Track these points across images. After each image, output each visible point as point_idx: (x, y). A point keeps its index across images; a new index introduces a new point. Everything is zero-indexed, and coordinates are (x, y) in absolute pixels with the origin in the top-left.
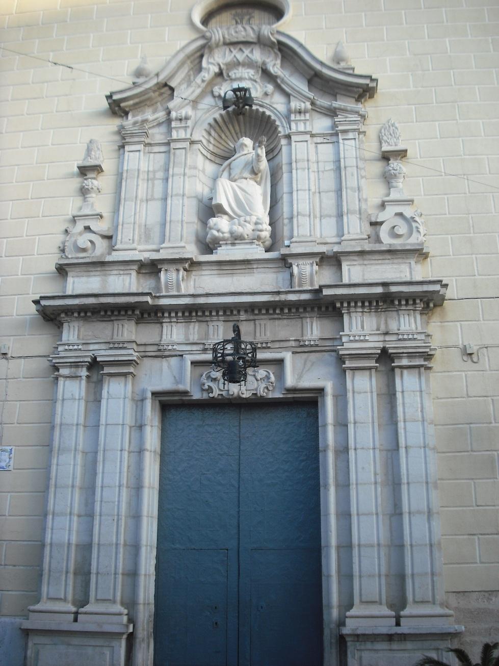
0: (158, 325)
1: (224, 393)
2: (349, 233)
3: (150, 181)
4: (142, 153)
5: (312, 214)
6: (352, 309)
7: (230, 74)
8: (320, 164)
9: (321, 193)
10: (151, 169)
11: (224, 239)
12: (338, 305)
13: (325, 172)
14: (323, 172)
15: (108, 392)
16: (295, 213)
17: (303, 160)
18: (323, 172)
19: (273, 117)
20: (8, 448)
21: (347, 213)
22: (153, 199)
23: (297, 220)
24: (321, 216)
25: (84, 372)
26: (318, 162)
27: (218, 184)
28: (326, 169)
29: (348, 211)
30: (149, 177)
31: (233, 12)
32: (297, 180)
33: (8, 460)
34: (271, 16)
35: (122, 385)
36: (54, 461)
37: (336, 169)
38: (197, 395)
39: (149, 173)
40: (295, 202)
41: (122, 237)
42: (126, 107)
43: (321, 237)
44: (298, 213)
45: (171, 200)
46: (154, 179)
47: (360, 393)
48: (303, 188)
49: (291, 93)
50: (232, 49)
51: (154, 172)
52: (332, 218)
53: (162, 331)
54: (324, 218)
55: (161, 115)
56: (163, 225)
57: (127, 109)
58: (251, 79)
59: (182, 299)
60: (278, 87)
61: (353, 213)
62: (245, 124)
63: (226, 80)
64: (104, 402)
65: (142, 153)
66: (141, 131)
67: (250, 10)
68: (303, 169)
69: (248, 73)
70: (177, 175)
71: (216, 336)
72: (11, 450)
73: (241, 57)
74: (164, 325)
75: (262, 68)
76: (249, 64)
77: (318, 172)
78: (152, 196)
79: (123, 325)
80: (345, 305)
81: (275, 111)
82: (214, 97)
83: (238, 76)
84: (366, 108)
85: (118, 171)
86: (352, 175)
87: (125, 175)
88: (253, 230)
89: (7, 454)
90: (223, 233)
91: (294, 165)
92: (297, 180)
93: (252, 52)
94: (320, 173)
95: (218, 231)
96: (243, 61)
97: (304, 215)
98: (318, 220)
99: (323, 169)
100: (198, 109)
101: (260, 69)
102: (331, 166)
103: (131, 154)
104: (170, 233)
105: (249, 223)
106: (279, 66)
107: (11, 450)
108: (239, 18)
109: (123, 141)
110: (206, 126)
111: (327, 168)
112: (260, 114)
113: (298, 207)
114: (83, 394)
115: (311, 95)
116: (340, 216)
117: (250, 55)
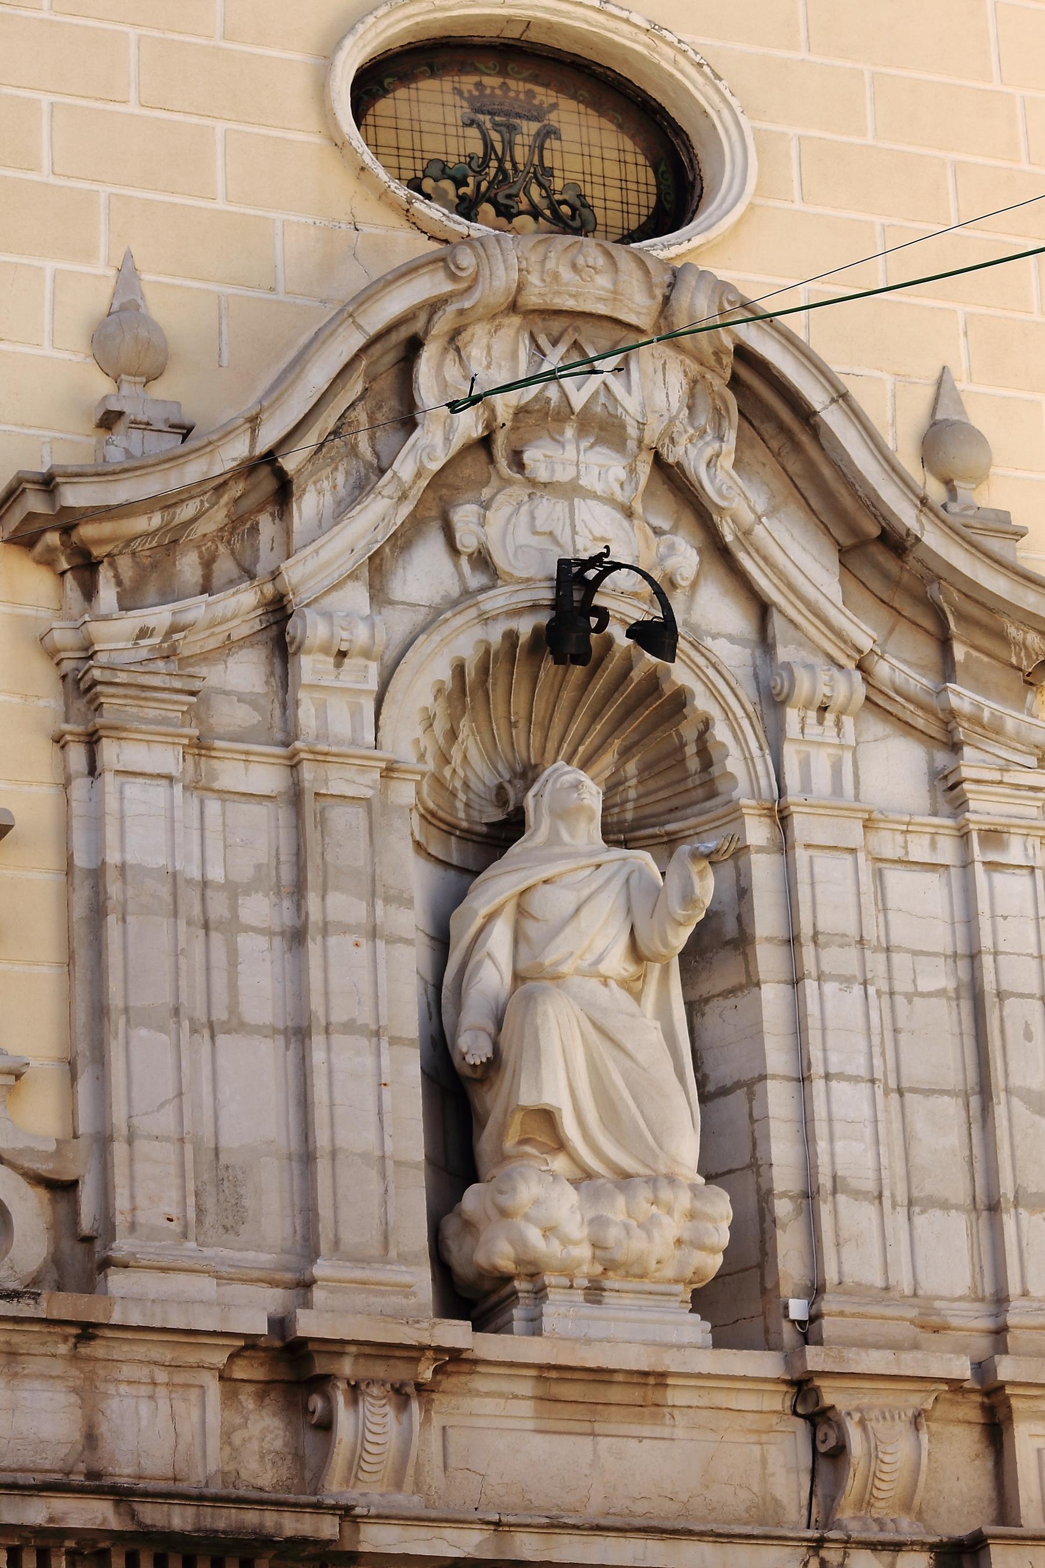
2: (1025, 1294)
4: (178, 788)
5: (886, 1193)
7: (528, 457)
8: (896, 957)
9: (908, 1096)
10: (216, 874)
11: (567, 1271)
13: (916, 999)
14: (909, 997)
16: (824, 1180)
17: (841, 939)
18: (909, 997)
19: (702, 703)
22: (238, 1026)
23: (835, 1212)
24: (910, 1203)
26: (888, 950)
27: (545, 1013)
29: (1016, 1198)
31: (468, 82)
32: (824, 1029)
34: (605, 123)
37: (957, 990)
39: (209, 893)
40: (821, 1128)
41: (132, 1197)
42: (100, 542)
43: (915, 1295)
44: (834, 1178)
45: (329, 1049)
46: (233, 926)
48: (850, 1070)
50: (543, 341)
51: (233, 890)
54: (923, 1212)
57: (97, 552)
58: (610, 500)
59: (450, 1533)
62: (595, 716)
63: (508, 482)
65: (178, 788)
66: (178, 684)
67: (544, 96)
68: (846, 980)
70: (345, 929)
77: (892, 994)
78: (233, 1008)
81: (711, 672)
83: (563, 475)
85: (69, 869)
86: (1028, 1036)
87: (114, 889)
88: (679, 1242)
90: (566, 1241)
91: (808, 952)
92: (824, 1029)
94: (900, 1000)
95: (549, 1231)
96: (586, 407)
97: (857, 1194)
98: (902, 1211)
99: (910, 988)
100: (391, 603)
101: (649, 457)
103: (134, 789)
104: (336, 1207)
105: (669, 1211)
106: (727, 462)
108: (496, 126)
110: (427, 698)
111: (925, 985)
112: (668, 690)
113: (832, 1155)
115: (864, 635)
117: (616, 384)
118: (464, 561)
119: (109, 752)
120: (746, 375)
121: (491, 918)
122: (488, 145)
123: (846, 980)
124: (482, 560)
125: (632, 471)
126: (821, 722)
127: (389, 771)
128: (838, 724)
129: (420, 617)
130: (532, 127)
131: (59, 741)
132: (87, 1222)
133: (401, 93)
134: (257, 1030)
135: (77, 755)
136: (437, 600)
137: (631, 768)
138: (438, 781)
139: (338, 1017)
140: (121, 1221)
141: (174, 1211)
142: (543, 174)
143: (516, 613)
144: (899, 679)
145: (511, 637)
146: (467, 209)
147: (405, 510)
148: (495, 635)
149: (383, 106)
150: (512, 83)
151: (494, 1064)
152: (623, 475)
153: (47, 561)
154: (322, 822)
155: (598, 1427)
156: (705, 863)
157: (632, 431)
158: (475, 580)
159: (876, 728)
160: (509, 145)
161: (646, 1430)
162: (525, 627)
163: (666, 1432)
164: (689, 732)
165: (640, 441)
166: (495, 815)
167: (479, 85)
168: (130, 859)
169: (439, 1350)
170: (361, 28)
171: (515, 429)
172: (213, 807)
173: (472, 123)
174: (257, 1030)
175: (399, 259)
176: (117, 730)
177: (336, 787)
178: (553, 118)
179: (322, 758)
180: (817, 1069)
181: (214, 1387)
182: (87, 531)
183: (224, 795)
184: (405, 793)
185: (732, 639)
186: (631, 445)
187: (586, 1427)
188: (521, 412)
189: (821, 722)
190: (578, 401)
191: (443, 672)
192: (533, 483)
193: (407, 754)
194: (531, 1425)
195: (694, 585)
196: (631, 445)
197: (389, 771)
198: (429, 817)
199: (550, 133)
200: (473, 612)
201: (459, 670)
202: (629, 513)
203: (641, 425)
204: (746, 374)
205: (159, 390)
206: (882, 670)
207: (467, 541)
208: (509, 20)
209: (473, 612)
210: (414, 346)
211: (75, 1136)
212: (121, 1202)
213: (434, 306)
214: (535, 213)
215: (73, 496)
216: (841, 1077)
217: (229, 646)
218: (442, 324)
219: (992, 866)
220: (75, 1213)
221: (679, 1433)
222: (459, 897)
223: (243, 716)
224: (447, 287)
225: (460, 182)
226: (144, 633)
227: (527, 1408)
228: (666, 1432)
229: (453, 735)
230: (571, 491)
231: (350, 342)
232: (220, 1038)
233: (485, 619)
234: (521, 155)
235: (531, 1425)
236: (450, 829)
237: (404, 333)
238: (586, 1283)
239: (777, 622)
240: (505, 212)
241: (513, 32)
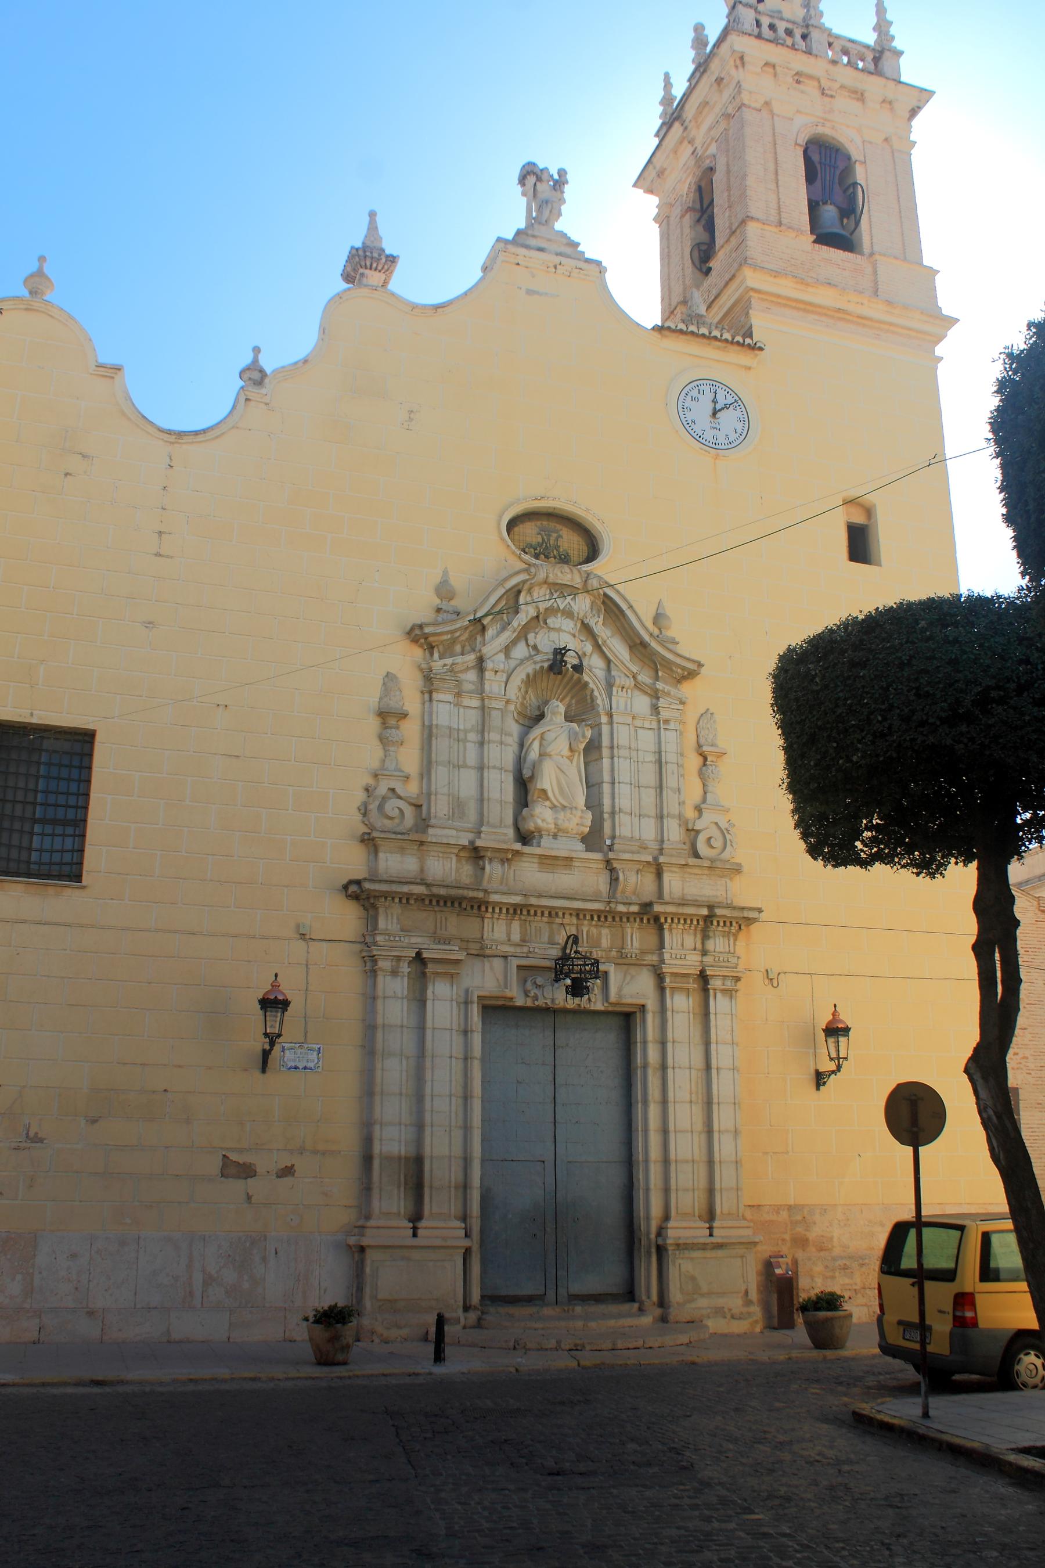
0: (478, 919)
1: (549, 1002)
2: (669, 840)
3: (461, 743)
4: (452, 705)
6: (674, 925)
8: (639, 752)
10: (461, 727)
11: (548, 831)
12: (662, 920)
15: (433, 993)
16: (617, 809)
19: (592, 685)
20: (316, 1047)
21: (668, 817)
22: (465, 766)
25: (405, 968)
28: (646, 760)
30: (460, 738)
31: (539, 523)
33: (316, 1061)
34: (575, 534)
35: (448, 985)
36: (379, 1066)
38: (520, 1002)
39: (460, 732)
40: (617, 796)
42: (434, 642)
46: (465, 740)
47: (678, 1012)
49: (614, 660)
51: (466, 731)
52: (651, 819)
53: (483, 928)
55: (471, 658)
56: (481, 800)
57: (434, 644)
58: (569, 633)
59: (513, 897)
60: (598, 647)
61: (673, 817)
62: (565, 688)
63: (543, 627)
64: (429, 1003)
65: (452, 705)
66: (453, 679)
67: (559, 527)
68: (626, 758)
69: (568, 625)
70: (494, 742)
71: (538, 939)
72: (319, 1048)
73: (562, 604)
74: (486, 920)
75: (582, 621)
76: (568, 614)
78: (464, 761)
79: (446, 919)
80: (669, 920)
81: (594, 677)
82: (528, 645)
83: (557, 626)
84: (687, 689)
85: (423, 725)
86: (673, 773)
87: (434, 731)
88: (577, 824)
89: (315, 1053)
90: (547, 823)
91: (616, 751)
93: (574, 599)
95: (543, 820)
97: (626, 813)
98: (637, 818)
100: (511, 658)
102: (651, 758)
103: (441, 705)
104: (488, 813)
105: (575, 816)
107: (319, 1048)
108: (546, 535)
109: (429, 683)
111: (647, 759)
112: (583, 682)
114: (406, 993)
116: (661, 817)
117: (572, 603)
118: (530, 648)
119: (435, 695)
120: (606, 600)
121: (534, 740)
122: (543, 540)
123: (626, 758)
124: (535, 647)
125: (576, 625)
126: (622, 691)
127: (508, 702)
128: (627, 692)
129: (518, 662)
130: (554, 535)
131: (422, 692)
132: (424, 815)
133: (521, 526)
134: (470, 767)
135: (427, 696)
136: (523, 658)
137: (574, 701)
138: (522, 704)
139: (491, 764)
140: (432, 815)
141: (446, 813)
142: (557, 548)
143: (543, 661)
144: (644, 680)
145: (542, 667)
146: (537, 556)
147: (515, 634)
148: (538, 667)
149: (516, 529)
150: (550, 524)
151: (532, 777)
152: (573, 626)
153: (421, 646)
154: (489, 715)
155: (555, 871)
156: (589, 727)
157: (576, 615)
158: (533, 653)
159: (637, 693)
160: (549, 540)
161: (568, 872)
162: (546, 665)
163: (572, 873)
164: (588, 692)
165: (578, 617)
166: (538, 713)
167: (542, 524)
168: (439, 723)
169: (512, 850)
170: (509, 509)
171: (545, 614)
172: (462, 710)
173: (539, 534)
174: (470, 767)
175: (517, 569)
176: (437, 690)
177: (493, 706)
178: (561, 533)
179: (490, 698)
180: (617, 781)
181: (454, 858)
182: (431, 639)
183: (465, 707)
184: (512, 707)
185: (600, 669)
186: (576, 618)
187: (551, 871)
188: (547, 609)
189: (622, 691)
190: (562, 607)
191: (524, 677)
192: (549, 628)
193: (513, 698)
194: (537, 870)
195: (591, 655)
196: (576, 618)
197: (508, 702)
198: (519, 713)
199: (560, 536)
200: (532, 661)
201: (528, 676)
202: (574, 636)
203: (578, 613)
204: (606, 600)
205: (453, 603)
206: (639, 678)
207: (531, 642)
208: (549, 507)
209: (532, 661)
210: (519, 592)
211: (422, 793)
212: (433, 810)
213: (524, 582)
214: (555, 557)
215: (427, 630)
216: (622, 783)
217: (468, 669)
218: (526, 587)
219: (666, 729)
220: (421, 813)
221: (576, 873)
222: (527, 733)
223: (471, 687)
224: (528, 577)
225: (535, 549)
226: (445, 665)
227: (536, 865)
228: (572, 873)
229: (527, 692)
230: (559, 630)
231: (501, 591)
232: (461, 769)
233: (535, 663)
234: (552, 542)
235: (537, 870)
236: (525, 716)
237: (516, 589)
238: (552, 834)
239: (612, 665)
240: (547, 557)
241: (550, 511)
